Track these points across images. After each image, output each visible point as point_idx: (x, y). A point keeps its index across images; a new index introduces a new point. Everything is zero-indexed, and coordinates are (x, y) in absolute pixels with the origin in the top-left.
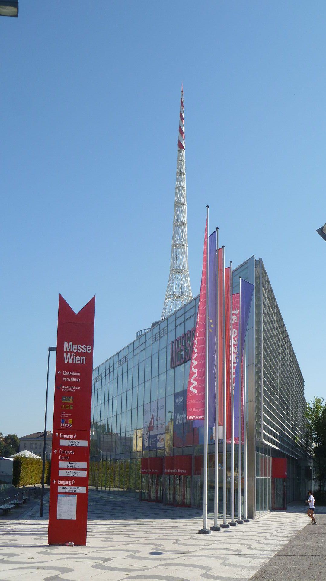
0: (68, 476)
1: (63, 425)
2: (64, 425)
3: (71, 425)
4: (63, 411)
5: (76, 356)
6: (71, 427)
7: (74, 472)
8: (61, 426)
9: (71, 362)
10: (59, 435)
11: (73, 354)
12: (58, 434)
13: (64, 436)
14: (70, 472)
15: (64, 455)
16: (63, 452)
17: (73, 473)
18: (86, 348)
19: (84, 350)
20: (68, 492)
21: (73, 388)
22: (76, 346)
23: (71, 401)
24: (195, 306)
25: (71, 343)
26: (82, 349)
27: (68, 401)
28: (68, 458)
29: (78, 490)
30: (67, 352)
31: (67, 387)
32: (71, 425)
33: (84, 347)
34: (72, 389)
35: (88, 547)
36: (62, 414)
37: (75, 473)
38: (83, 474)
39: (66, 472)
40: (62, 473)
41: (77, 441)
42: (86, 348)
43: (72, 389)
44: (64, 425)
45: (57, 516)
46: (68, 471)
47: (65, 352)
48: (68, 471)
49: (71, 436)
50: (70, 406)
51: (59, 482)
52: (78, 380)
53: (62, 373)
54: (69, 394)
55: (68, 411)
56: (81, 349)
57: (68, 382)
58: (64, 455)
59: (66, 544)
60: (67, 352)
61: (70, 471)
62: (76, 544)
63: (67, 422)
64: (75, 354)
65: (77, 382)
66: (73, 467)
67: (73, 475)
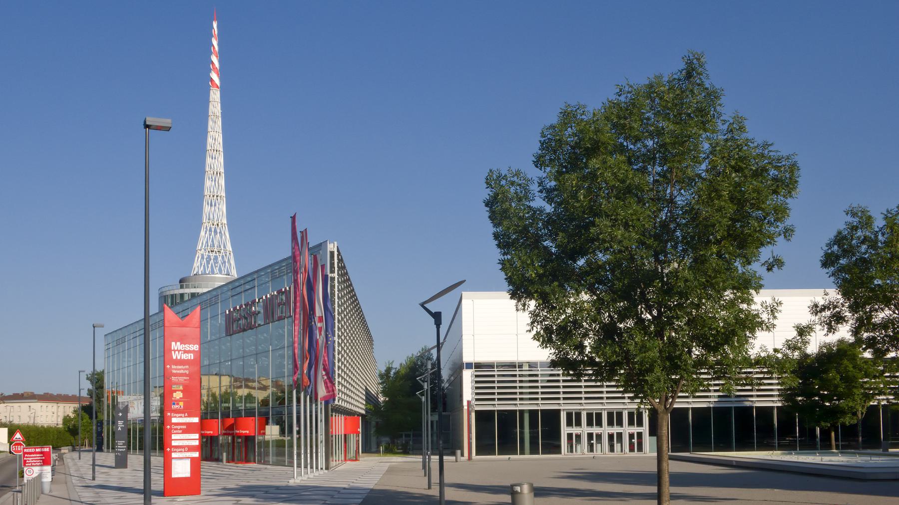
5: (184, 353)
11: (180, 352)
22: (183, 345)
25: (178, 343)
64: (183, 352)
65: (186, 373)
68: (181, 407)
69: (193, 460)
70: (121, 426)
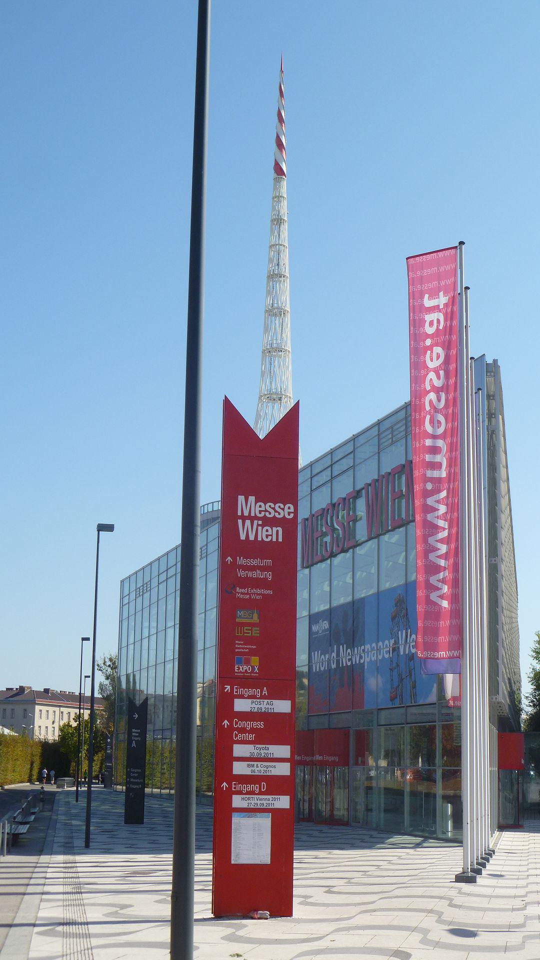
0: (253, 774)
1: (239, 668)
2: (241, 669)
3: (256, 668)
4: (239, 638)
5: (263, 526)
6: (256, 673)
7: (265, 766)
8: (236, 671)
9: (252, 538)
10: (232, 689)
11: (256, 522)
12: (229, 687)
13: (241, 691)
14: (255, 765)
15: (243, 730)
16: (241, 724)
17: (262, 769)
18: (283, 509)
19: (279, 514)
20: (252, 807)
21: (259, 591)
23: (255, 618)
24: (353, 452)
25: (252, 499)
26: (276, 511)
27: (246, 618)
28: (252, 737)
29: (273, 802)
30: (244, 518)
31: (245, 591)
32: (256, 668)
33: (279, 507)
34: (257, 593)
35: (299, 921)
36: (237, 646)
37: (267, 767)
38: (283, 769)
39: (249, 766)
40: (239, 768)
41: (269, 701)
42: (283, 509)
43: (257, 593)
44: (241, 669)
45: (232, 858)
46: (253, 763)
47: (240, 517)
48: (251, 763)
49: (257, 692)
50: (254, 629)
51: (233, 786)
52: (268, 575)
53: (235, 559)
54: (249, 604)
55: (248, 640)
56: (272, 511)
57: (247, 578)
58: (243, 730)
59: (251, 915)
60: (244, 518)
61: (255, 763)
62: (274, 915)
63: (247, 662)
64: (260, 522)
66: (263, 755)
67: (262, 772)
68: (253, 668)
69: (277, 815)
70: (136, 739)
